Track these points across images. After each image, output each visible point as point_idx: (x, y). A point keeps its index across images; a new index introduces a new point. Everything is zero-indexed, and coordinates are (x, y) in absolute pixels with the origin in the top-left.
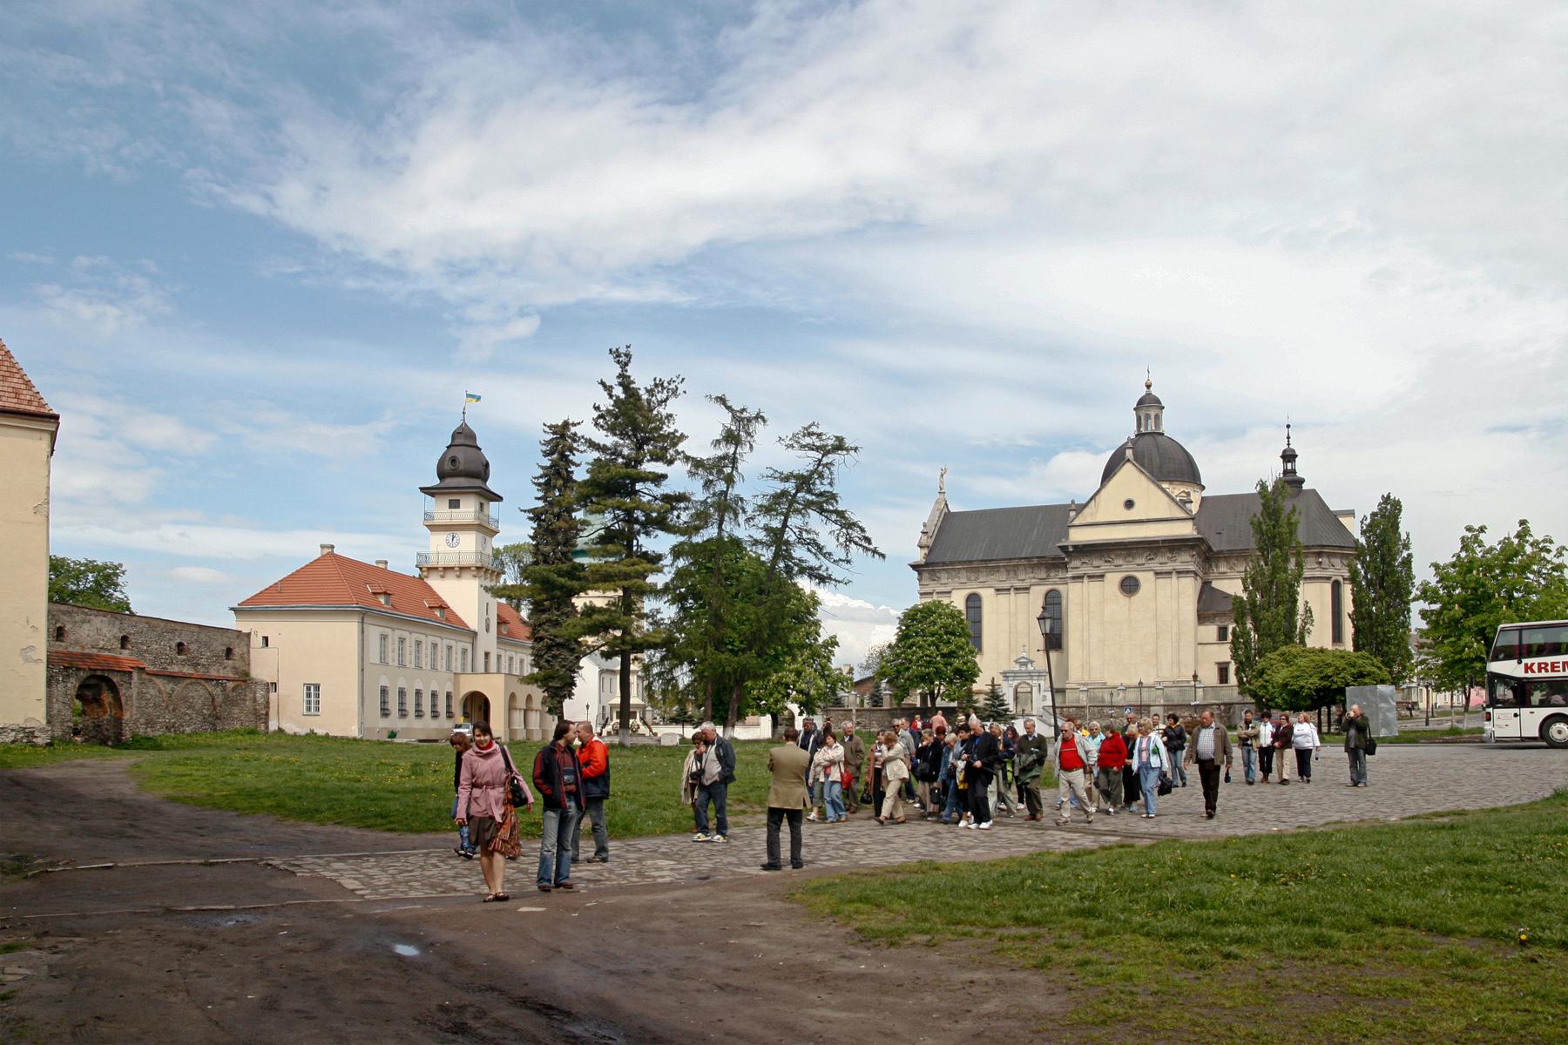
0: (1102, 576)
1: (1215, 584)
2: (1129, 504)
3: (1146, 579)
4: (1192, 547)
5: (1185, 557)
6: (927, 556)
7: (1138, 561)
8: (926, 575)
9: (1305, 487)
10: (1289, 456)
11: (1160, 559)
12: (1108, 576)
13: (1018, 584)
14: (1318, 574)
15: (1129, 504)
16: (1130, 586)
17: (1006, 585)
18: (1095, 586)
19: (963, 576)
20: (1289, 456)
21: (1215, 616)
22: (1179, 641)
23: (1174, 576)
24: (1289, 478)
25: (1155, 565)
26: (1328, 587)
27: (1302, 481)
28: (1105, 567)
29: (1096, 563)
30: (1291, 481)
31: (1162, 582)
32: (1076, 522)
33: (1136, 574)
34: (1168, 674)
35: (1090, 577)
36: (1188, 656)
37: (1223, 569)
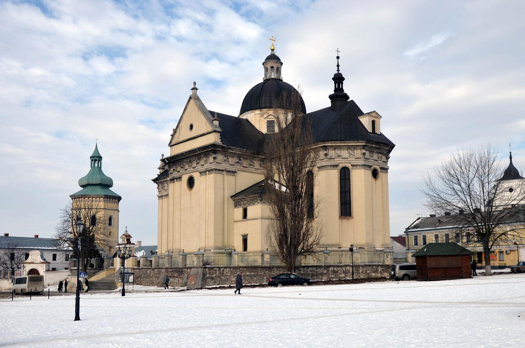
2: (191, 127)
7: (194, 165)
8: (160, 186)
10: (338, 79)
11: (202, 162)
15: (191, 127)
16: (191, 182)
20: (338, 79)
23: (207, 173)
24: (340, 94)
25: (199, 167)
28: (182, 171)
29: (179, 169)
30: (339, 97)
32: (173, 143)
35: (177, 179)
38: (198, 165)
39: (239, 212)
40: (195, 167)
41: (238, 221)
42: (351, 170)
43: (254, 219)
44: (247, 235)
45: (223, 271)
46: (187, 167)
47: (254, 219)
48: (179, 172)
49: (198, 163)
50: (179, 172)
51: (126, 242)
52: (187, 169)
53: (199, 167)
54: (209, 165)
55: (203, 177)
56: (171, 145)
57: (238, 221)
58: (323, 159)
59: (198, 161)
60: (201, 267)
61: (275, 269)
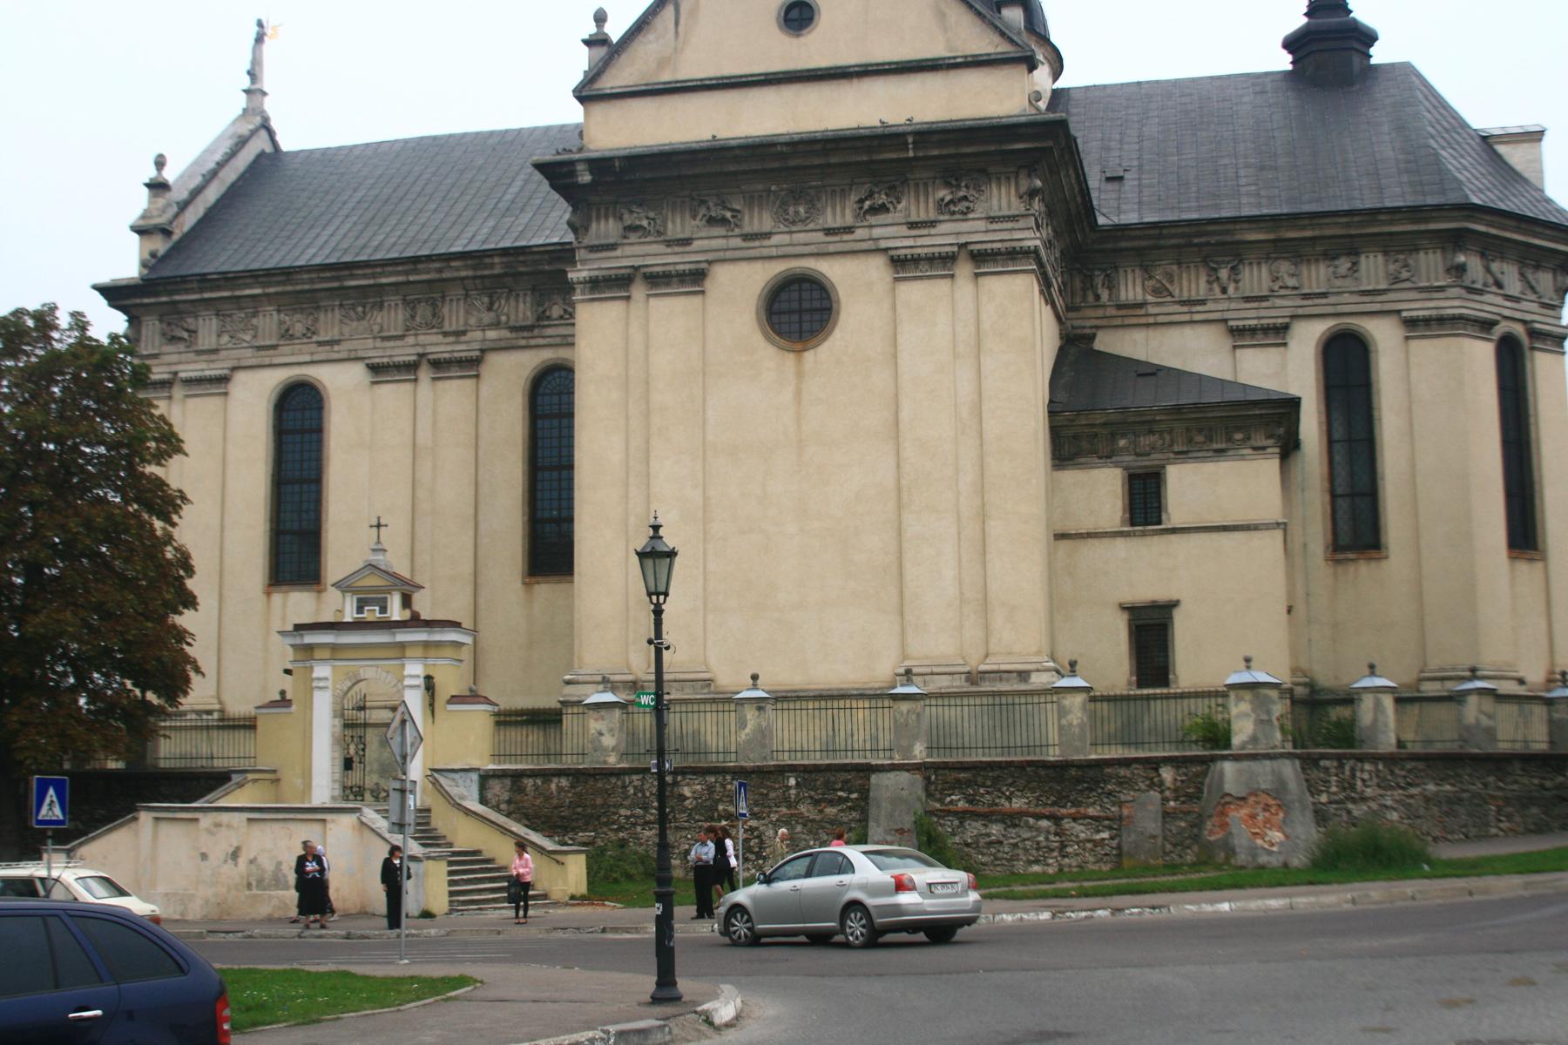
0: (694, 279)
1: (1107, 342)
3: (856, 281)
4: (1027, 163)
5: (1002, 198)
6: (152, 263)
7: (831, 219)
9: (1380, 55)
11: (914, 207)
12: (723, 277)
13: (439, 346)
14: (1453, 304)
16: (798, 312)
17: (403, 352)
18: (668, 315)
19: (268, 322)
21: (1116, 429)
22: (983, 516)
23: (964, 269)
25: (890, 231)
26: (1481, 355)
27: (1369, 38)
28: (709, 241)
29: (677, 226)
31: (915, 292)
32: (609, 83)
33: (832, 270)
34: (943, 642)
35: (659, 280)
36: (1020, 570)
37: (1132, 289)
38: (872, 220)
39: (1101, 490)
40: (849, 230)
41: (1090, 535)
42: (1527, 353)
43: (1225, 529)
44: (1169, 607)
45: (1353, 770)
46: (762, 220)
47: (1225, 529)
48: (687, 242)
49: (882, 209)
50: (687, 242)
51: (396, 612)
52: (768, 235)
53: (877, 232)
54: (981, 225)
55: (918, 293)
56: (587, 94)
57: (1090, 535)
58: (1441, 289)
59: (882, 199)
60: (1289, 756)
61: (1517, 767)
